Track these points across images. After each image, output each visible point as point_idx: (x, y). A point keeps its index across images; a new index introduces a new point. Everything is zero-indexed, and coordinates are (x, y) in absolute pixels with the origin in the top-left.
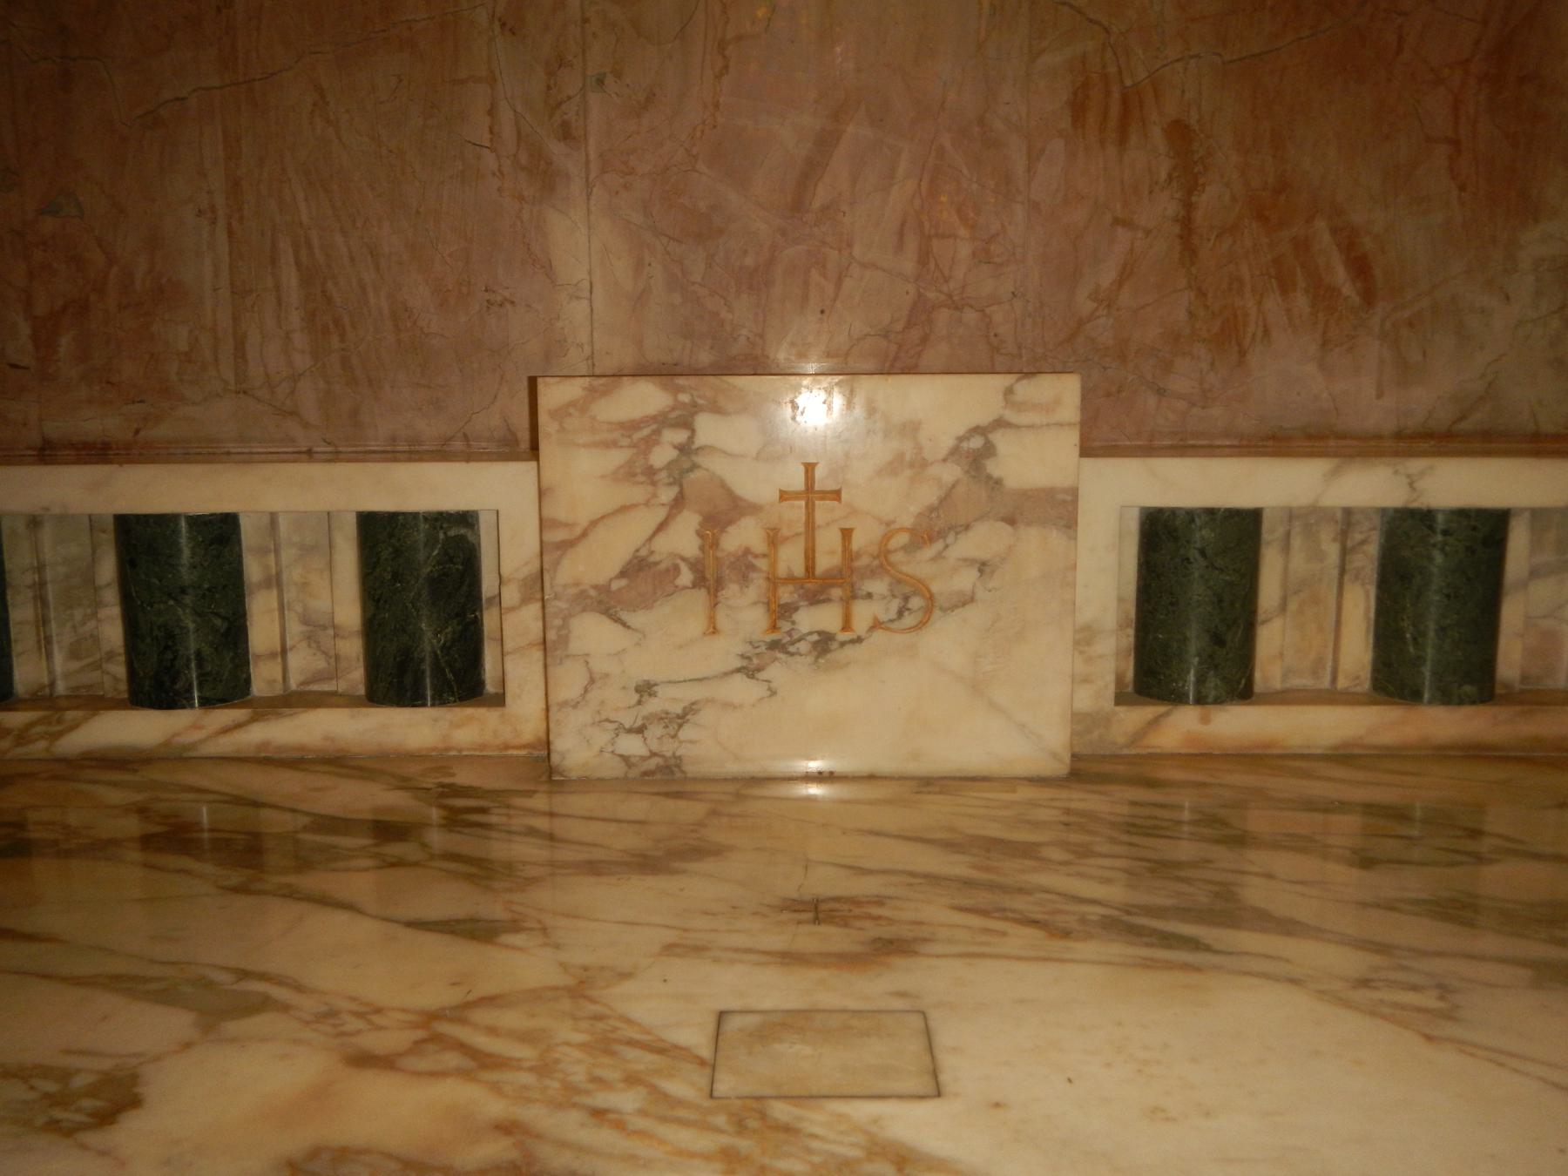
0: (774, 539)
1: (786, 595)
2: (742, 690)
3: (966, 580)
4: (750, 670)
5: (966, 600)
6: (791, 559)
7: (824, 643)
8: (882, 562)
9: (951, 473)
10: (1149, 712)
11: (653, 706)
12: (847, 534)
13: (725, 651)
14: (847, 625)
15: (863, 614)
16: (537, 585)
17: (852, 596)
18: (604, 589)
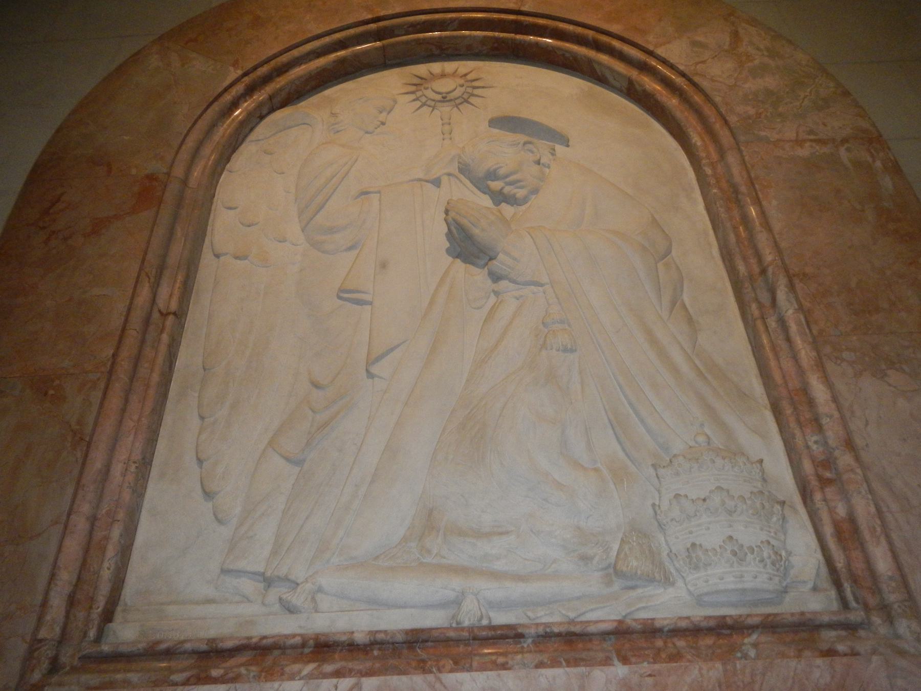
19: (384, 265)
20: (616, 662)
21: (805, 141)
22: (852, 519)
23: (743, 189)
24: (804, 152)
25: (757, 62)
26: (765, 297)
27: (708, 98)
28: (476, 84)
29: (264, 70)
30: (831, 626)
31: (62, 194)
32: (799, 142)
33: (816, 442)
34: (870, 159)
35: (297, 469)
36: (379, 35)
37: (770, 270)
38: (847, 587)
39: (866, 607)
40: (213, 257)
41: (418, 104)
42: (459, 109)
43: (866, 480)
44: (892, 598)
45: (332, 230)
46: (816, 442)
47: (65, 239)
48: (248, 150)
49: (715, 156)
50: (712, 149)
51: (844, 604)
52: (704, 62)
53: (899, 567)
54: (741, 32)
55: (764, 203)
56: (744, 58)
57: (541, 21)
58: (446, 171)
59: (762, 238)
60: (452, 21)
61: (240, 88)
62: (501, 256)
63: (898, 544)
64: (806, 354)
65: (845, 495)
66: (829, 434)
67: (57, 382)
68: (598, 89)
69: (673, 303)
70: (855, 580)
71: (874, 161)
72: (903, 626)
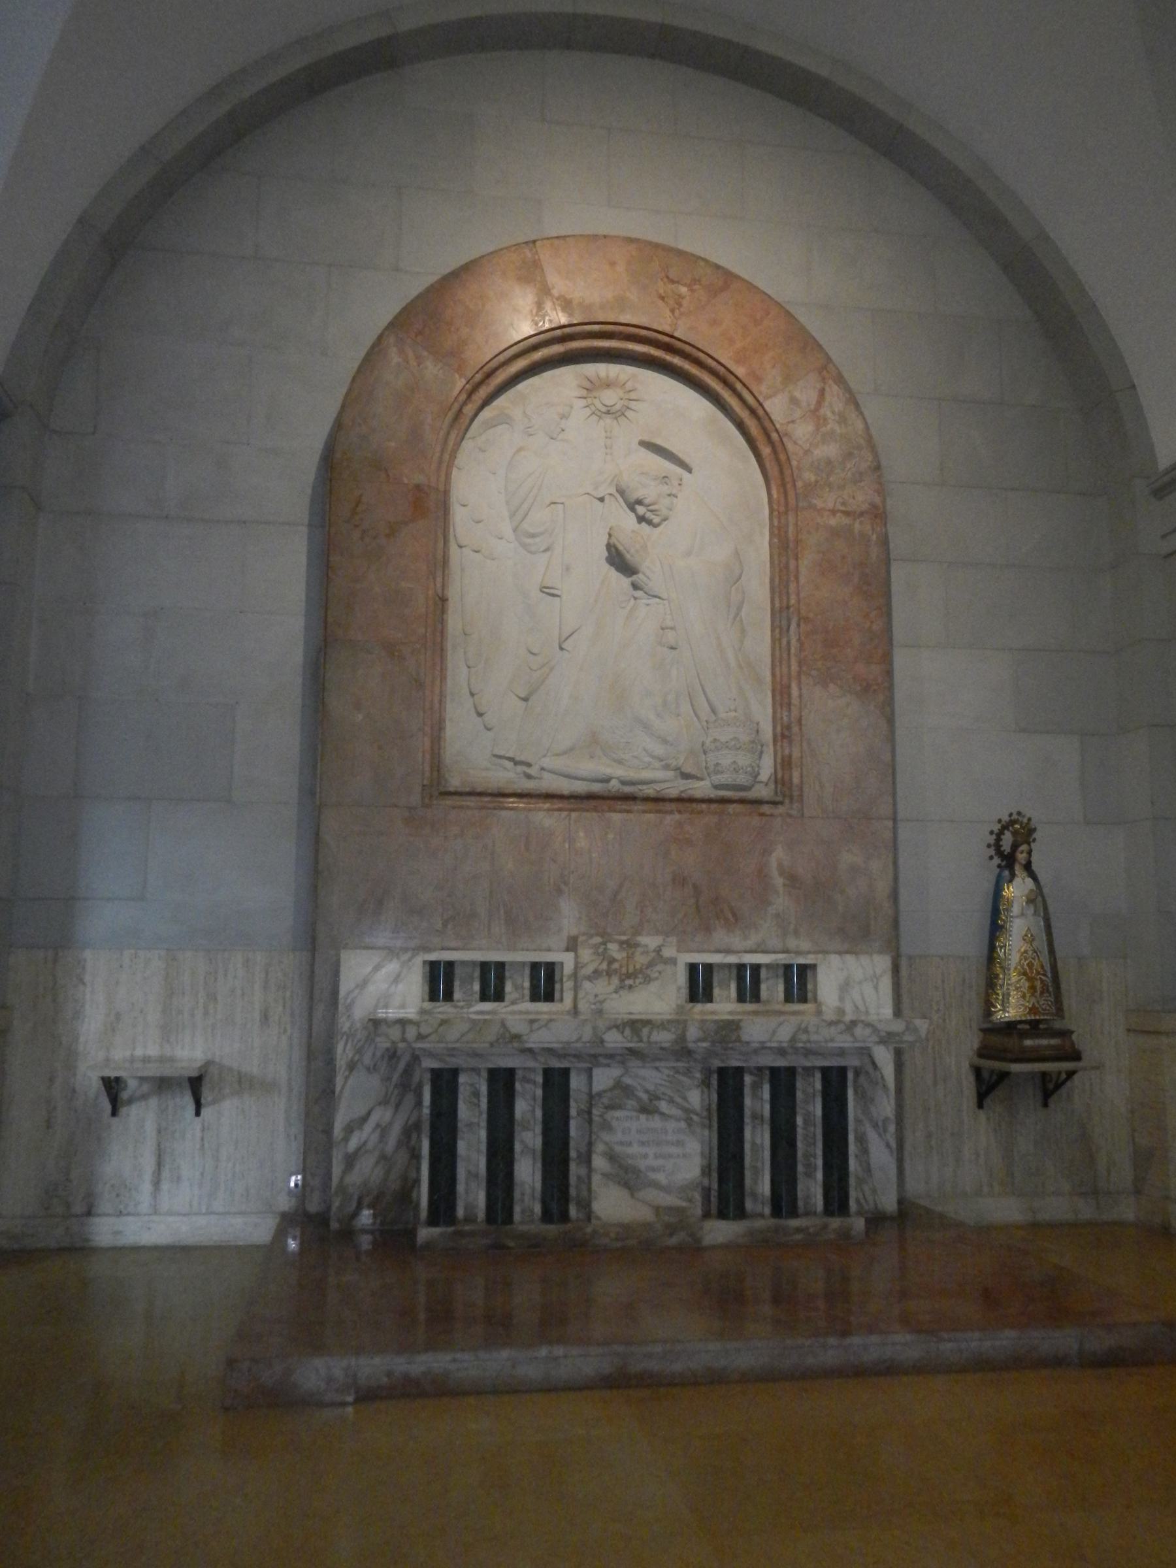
0: (621, 967)
1: (624, 977)
2: (614, 996)
3: (656, 975)
4: (616, 992)
5: (657, 979)
6: (624, 970)
7: (630, 987)
8: (641, 971)
9: (653, 955)
10: (691, 1005)
11: (598, 999)
12: (634, 967)
13: (612, 988)
14: (634, 983)
15: (638, 981)
16: (575, 975)
17: (636, 977)
18: (589, 976)
19: (568, 569)
20: (676, 813)
21: (839, 511)
22: (790, 756)
23: (791, 545)
24: (833, 522)
25: (829, 427)
26: (784, 623)
27: (788, 459)
28: (633, 395)
29: (478, 377)
30: (768, 802)
31: (361, 496)
32: (834, 512)
33: (787, 716)
34: (870, 533)
35: (523, 704)
36: (562, 339)
37: (792, 609)
38: (779, 786)
39: (784, 796)
40: (457, 547)
41: (588, 411)
42: (617, 421)
43: (801, 740)
44: (796, 793)
45: (533, 536)
46: (787, 716)
47: (375, 538)
48: (467, 444)
49: (782, 509)
50: (782, 500)
51: (776, 793)
52: (793, 422)
53: (802, 782)
54: (827, 389)
55: (800, 561)
56: (821, 421)
57: (687, 348)
58: (606, 493)
59: (792, 586)
60: (621, 333)
61: (464, 396)
62: (640, 576)
63: (805, 773)
64: (794, 667)
65: (790, 743)
66: (792, 714)
67: (397, 647)
68: (719, 415)
69: (735, 618)
70: (783, 784)
71: (873, 534)
72: (796, 805)
